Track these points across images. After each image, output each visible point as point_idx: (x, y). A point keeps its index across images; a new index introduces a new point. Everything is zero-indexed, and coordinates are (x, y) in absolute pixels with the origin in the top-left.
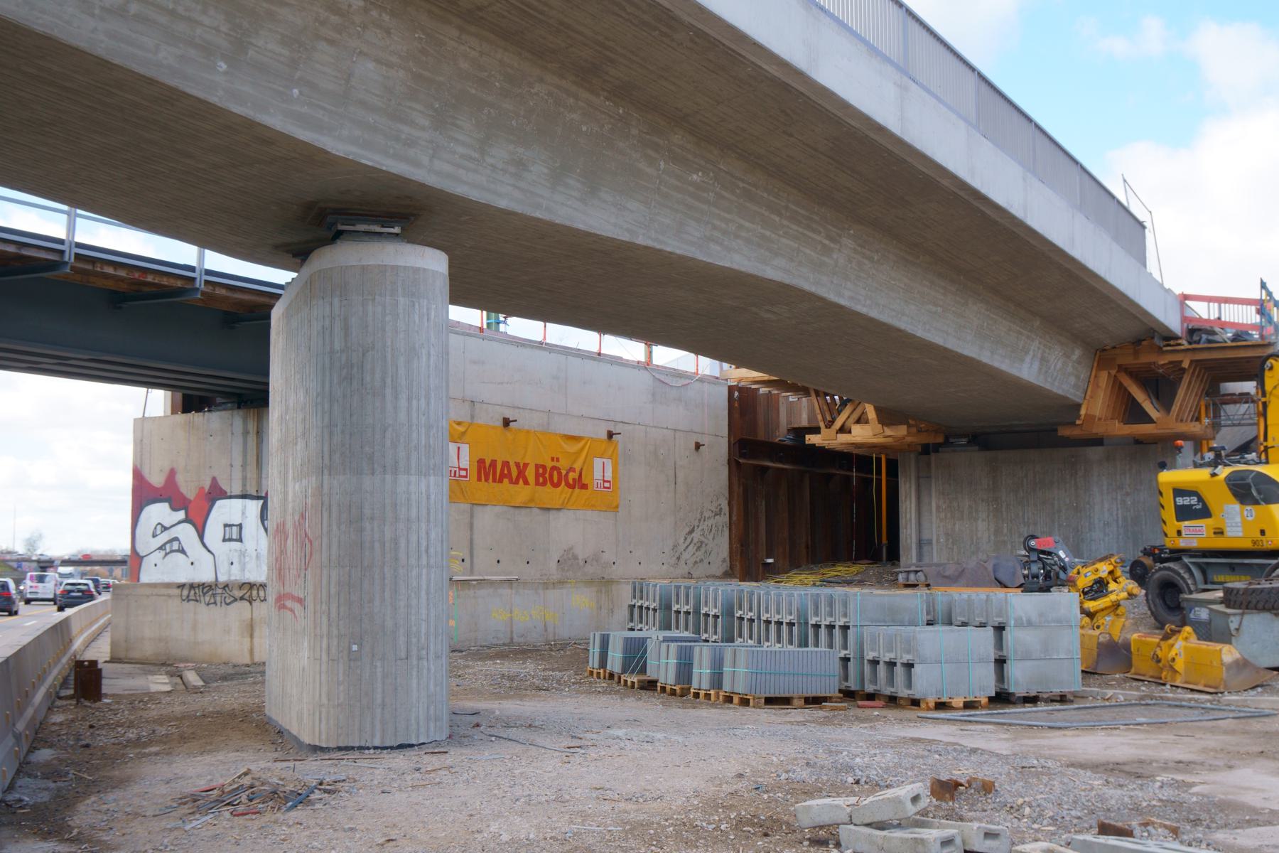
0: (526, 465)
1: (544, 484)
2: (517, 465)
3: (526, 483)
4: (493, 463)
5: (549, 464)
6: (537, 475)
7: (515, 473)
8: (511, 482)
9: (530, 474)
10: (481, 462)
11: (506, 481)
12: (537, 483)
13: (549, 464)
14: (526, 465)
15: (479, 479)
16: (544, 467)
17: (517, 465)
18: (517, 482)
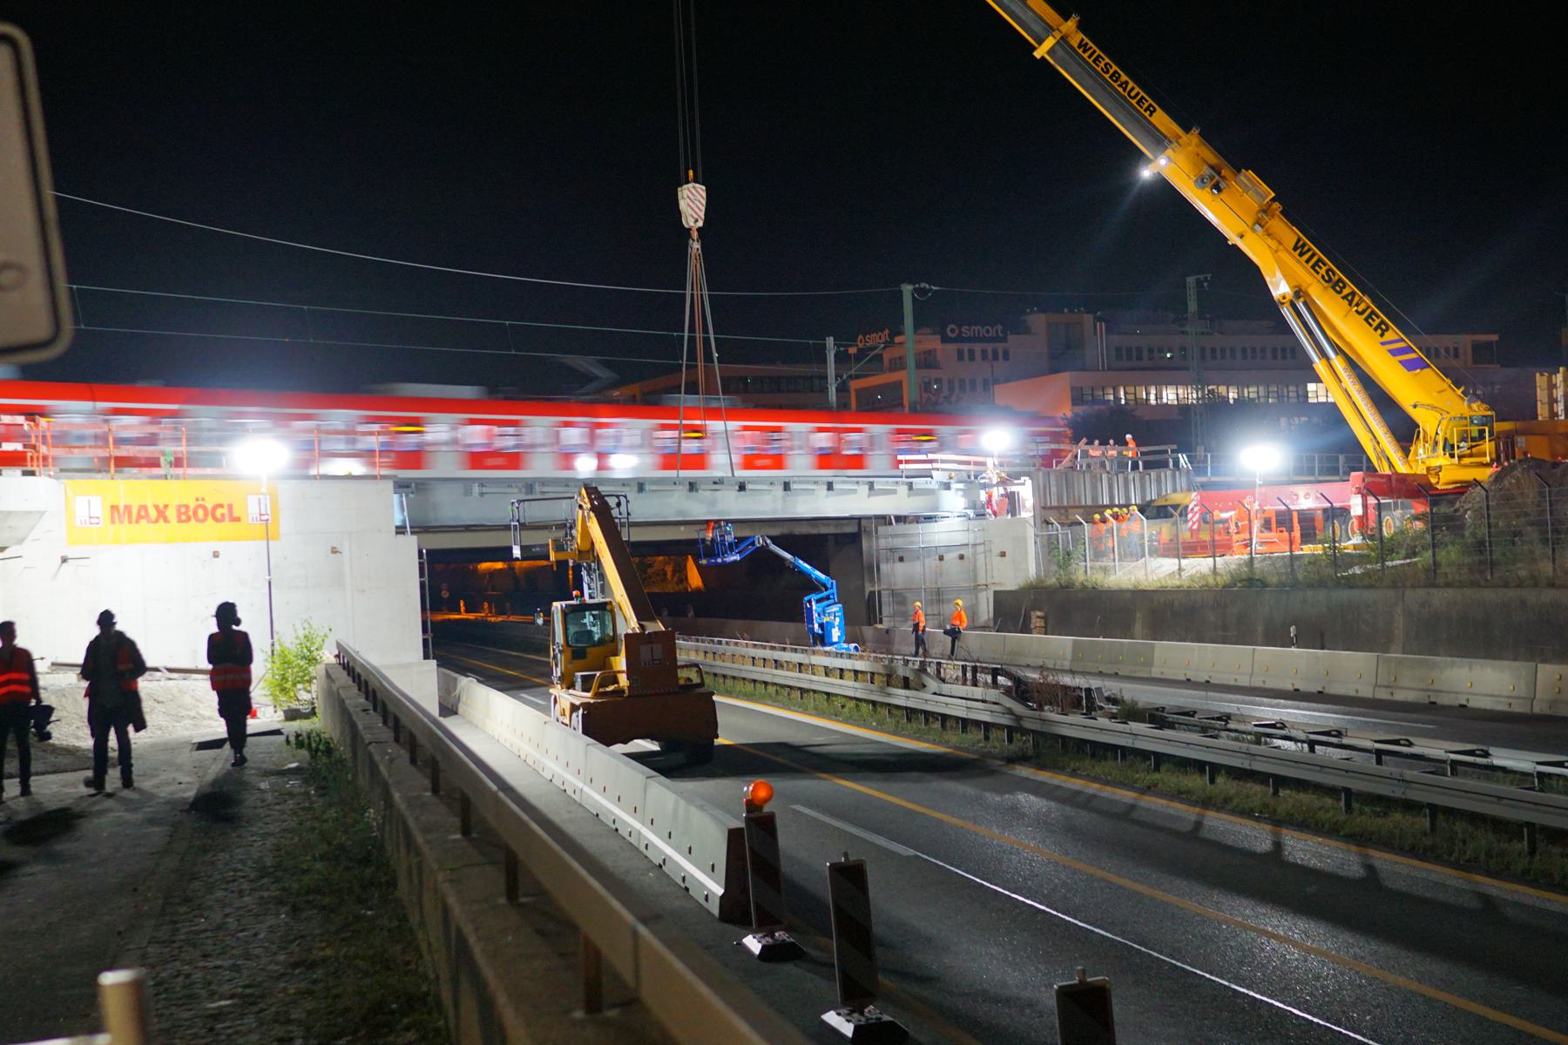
0: (166, 506)
1: (188, 519)
2: (157, 507)
3: (166, 520)
4: (128, 508)
5: (192, 504)
6: (179, 514)
7: (153, 513)
8: (150, 521)
9: (171, 513)
10: (114, 508)
11: (143, 521)
12: (180, 521)
13: (192, 504)
14: (166, 506)
15: (113, 521)
16: (187, 507)
17: (157, 507)
18: (156, 521)
